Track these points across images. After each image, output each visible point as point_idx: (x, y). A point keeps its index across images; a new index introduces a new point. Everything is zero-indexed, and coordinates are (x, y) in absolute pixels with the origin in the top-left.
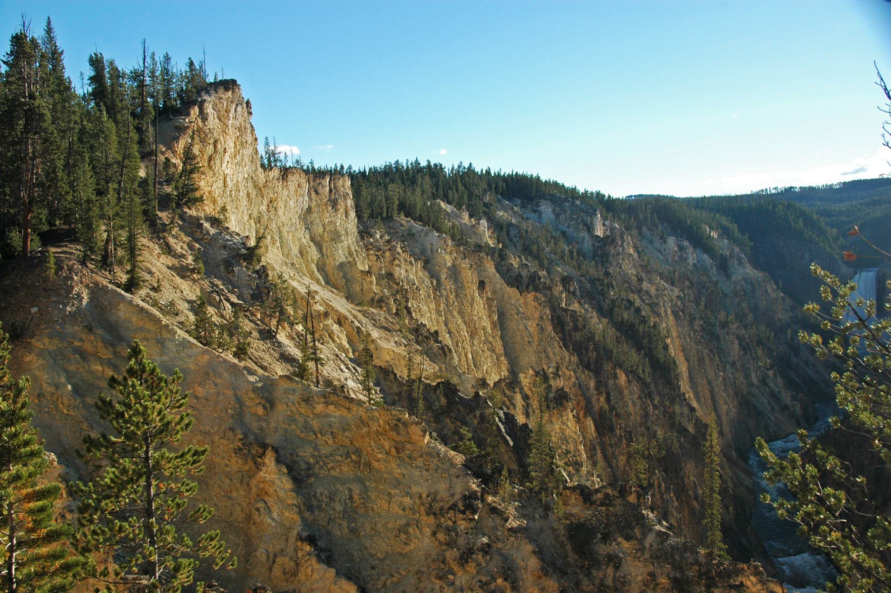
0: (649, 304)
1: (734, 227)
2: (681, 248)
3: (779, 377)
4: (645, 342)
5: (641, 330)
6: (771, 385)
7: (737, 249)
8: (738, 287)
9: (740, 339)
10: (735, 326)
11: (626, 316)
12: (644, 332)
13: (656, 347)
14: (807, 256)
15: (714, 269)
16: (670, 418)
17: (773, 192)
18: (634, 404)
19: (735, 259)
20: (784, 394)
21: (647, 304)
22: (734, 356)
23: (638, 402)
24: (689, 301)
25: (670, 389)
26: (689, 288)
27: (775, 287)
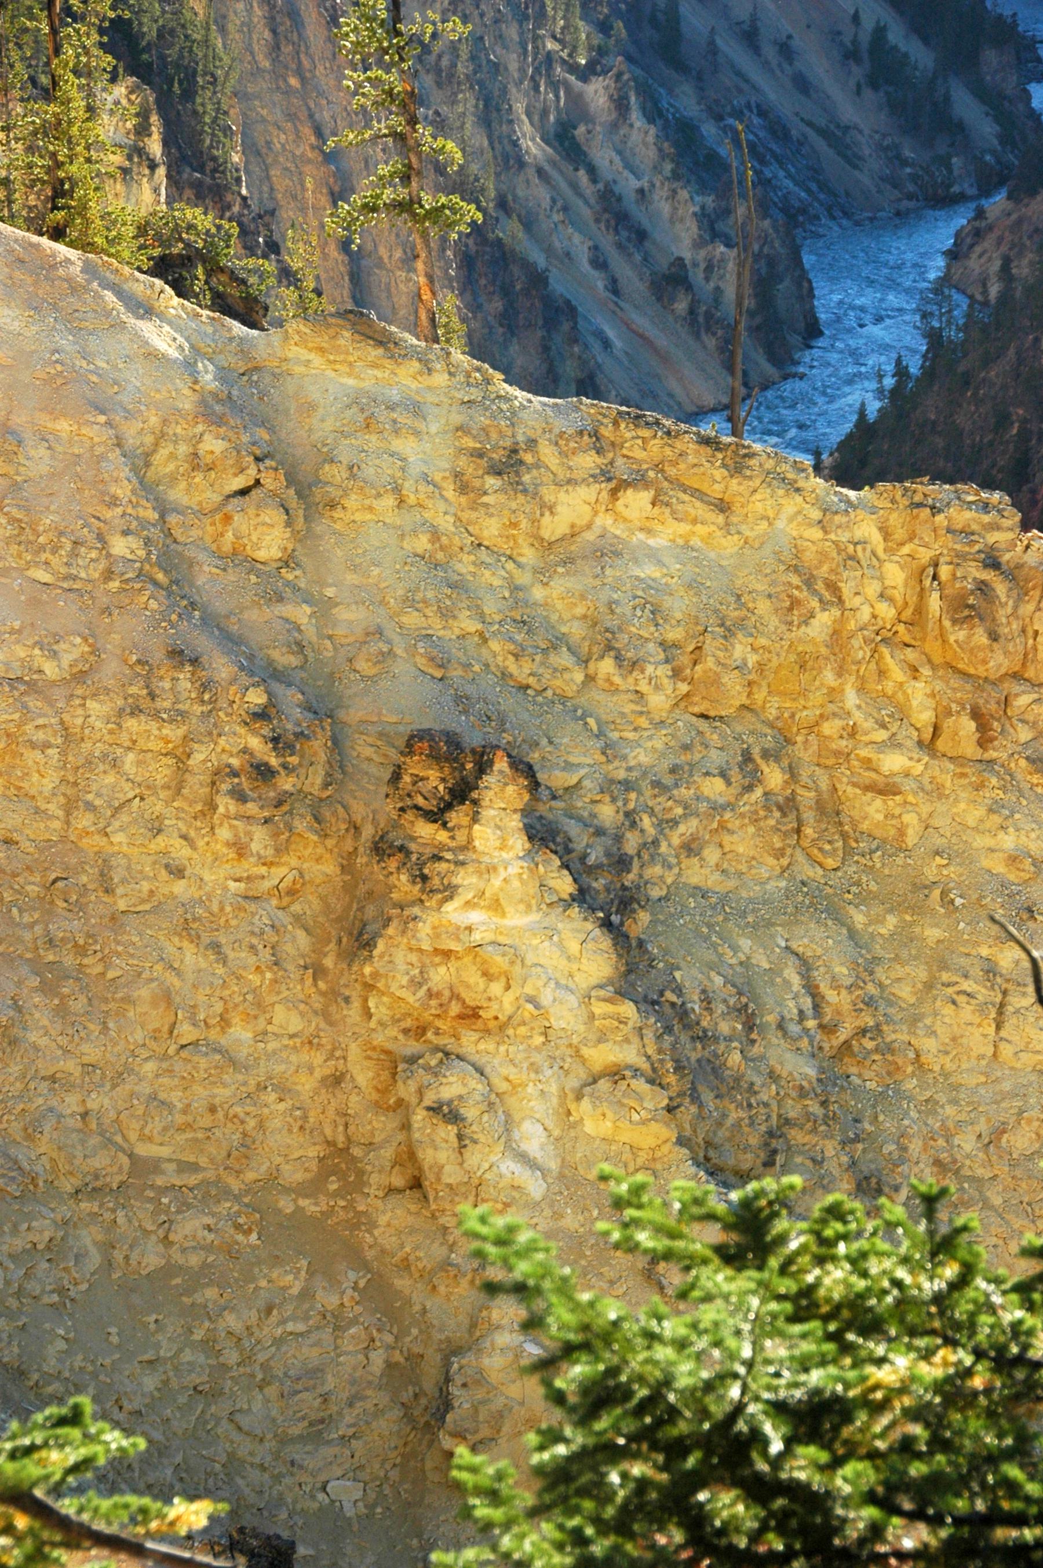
3: (636, 117)
20: (665, 208)
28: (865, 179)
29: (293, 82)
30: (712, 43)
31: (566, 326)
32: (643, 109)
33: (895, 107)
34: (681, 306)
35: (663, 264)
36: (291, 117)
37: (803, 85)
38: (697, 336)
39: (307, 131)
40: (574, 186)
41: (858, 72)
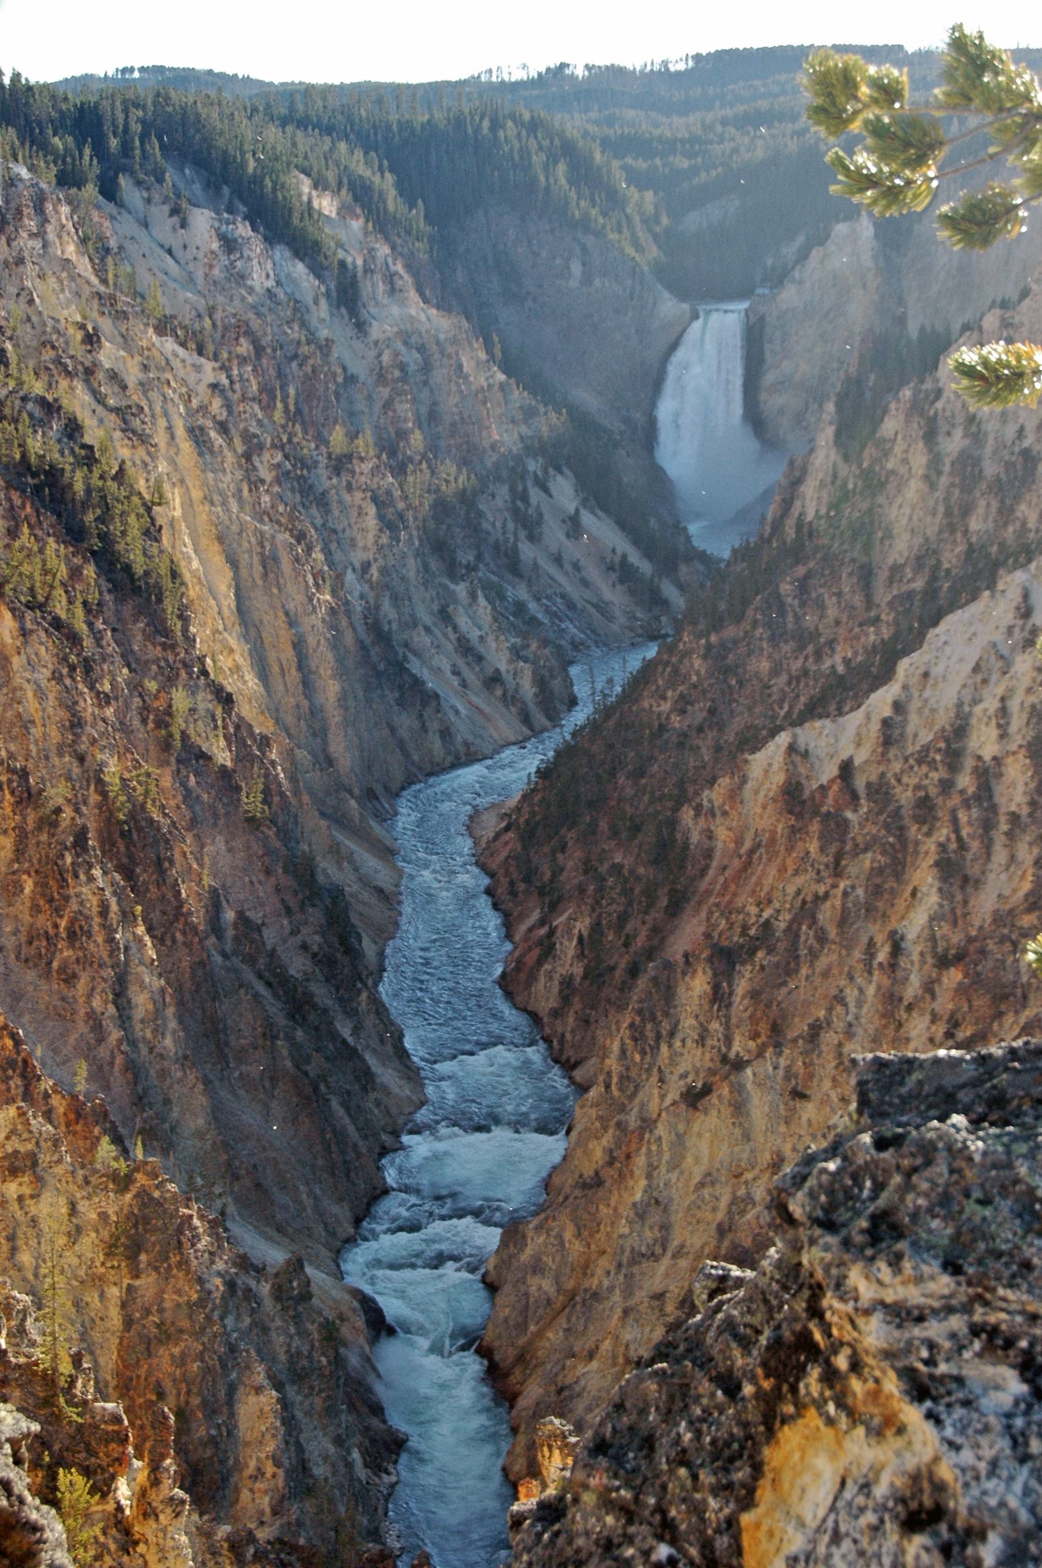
0: (117, 410)
1: (386, 184)
2: (230, 244)
3: (482, 601)
4: (89, 517)
5: (79, 487)
6: (463, 621)
7: (383, 250)
8: (386, 358)
9: (382, 501)
10: (367, 467)
11: (35, 444)
12: (88, 491)
13: (124, 533)
14: (576, 268)
15: (323, 302)
16: (159, 724)
17: (519, 75)
18: (40, 694)
19: (378, 277)
20: (494, 645)
21: (111, 410)
22: (365, 548)
23: (53, 691)
24: (244, 398)
25: (164, 647)
26: (243, 360)
27: (483, 356)
28: (615, 627)
29: (275, 591)
30: (535, 564)
31: (434, 704)
32: (486, 597)
33: (632, 593)
34: (499, 692)
35: (489, 671)
36: (273, 607)
37: (585, 583)
38: (507, 707)
39: (281, 614)
40: (445, 635)
41: (614, 576)
